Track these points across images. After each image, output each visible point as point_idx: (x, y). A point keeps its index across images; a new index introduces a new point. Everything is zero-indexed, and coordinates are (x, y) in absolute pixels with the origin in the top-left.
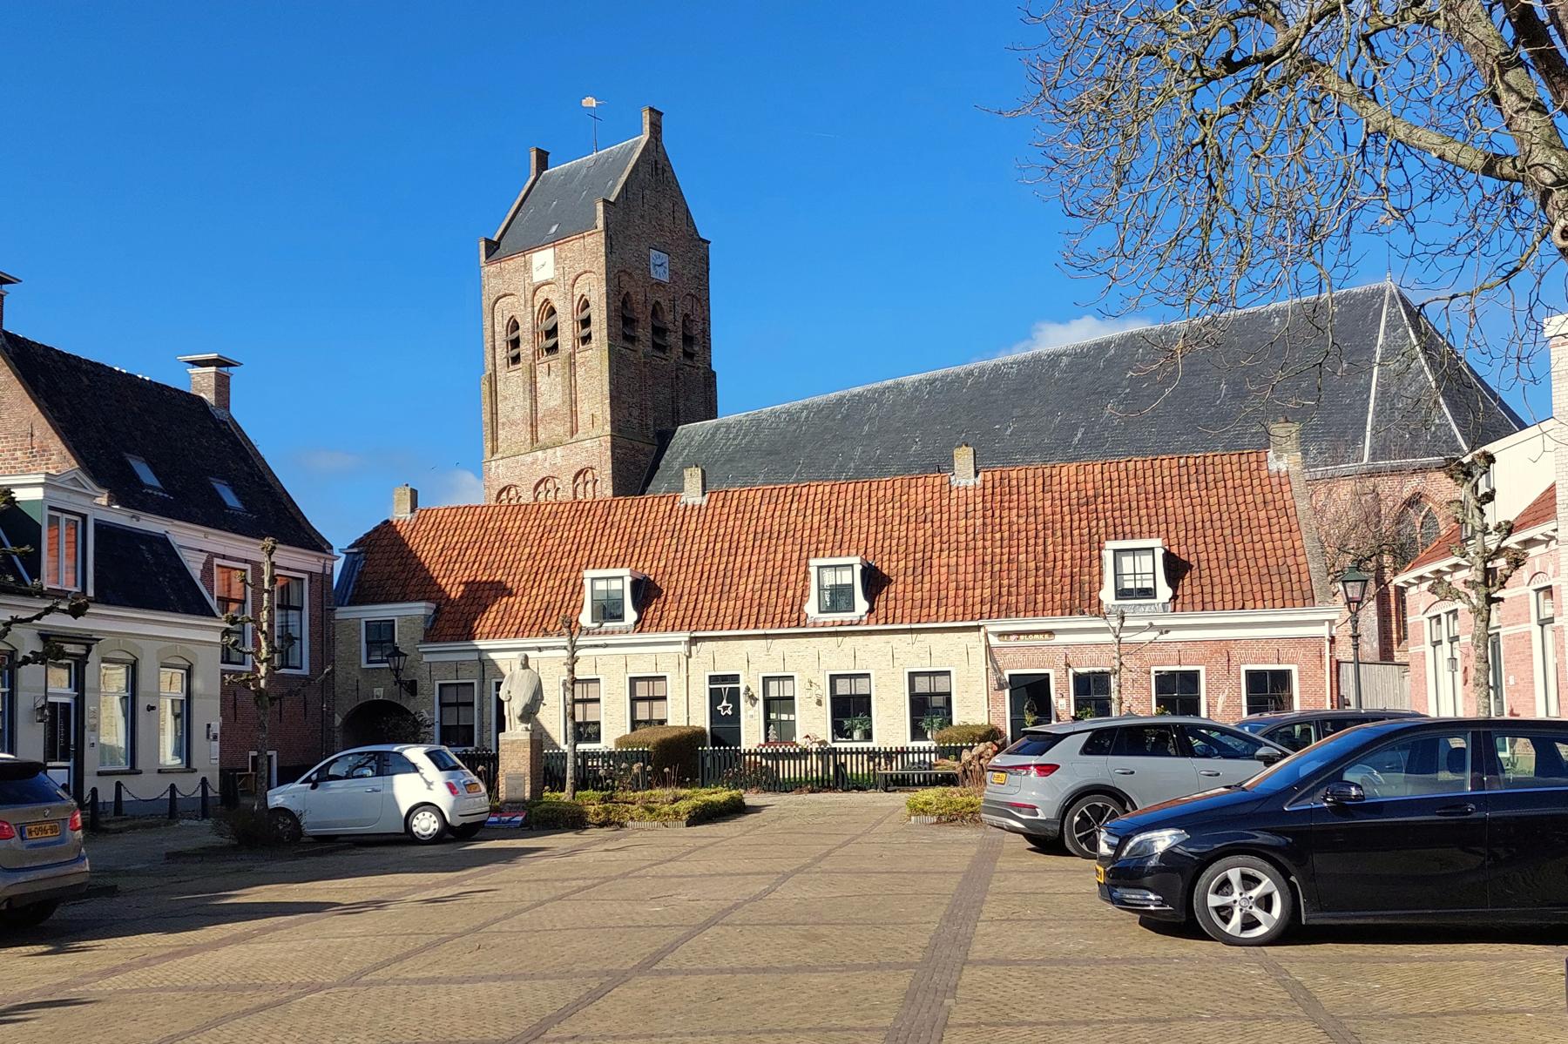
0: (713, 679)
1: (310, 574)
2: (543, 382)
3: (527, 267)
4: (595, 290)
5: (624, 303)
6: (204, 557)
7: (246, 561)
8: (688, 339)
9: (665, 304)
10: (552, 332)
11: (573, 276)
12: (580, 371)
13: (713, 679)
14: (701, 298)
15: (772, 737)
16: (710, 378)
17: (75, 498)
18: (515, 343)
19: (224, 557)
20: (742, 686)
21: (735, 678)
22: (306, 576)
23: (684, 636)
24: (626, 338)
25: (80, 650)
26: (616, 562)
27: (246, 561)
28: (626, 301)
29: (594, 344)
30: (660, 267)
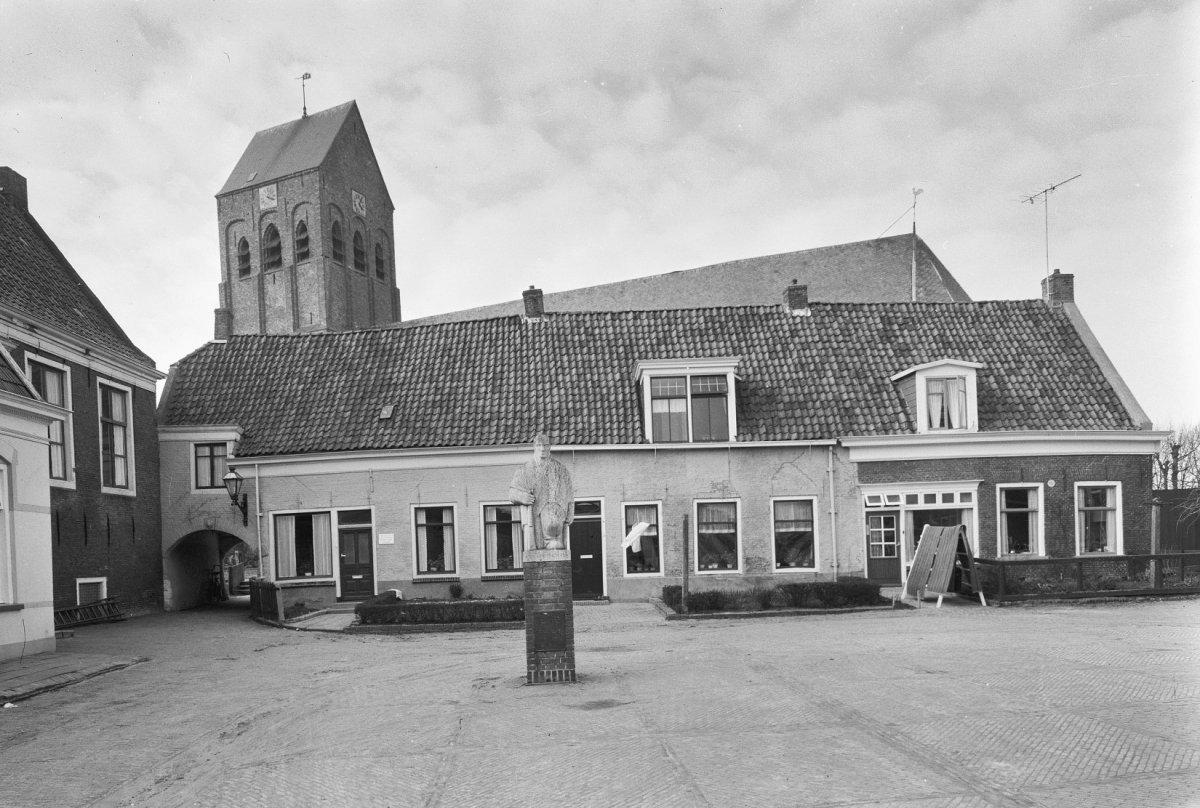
2: (270, 288)
4: (312, 215)
5: (334, 230)
7: (64, 361)
8: (379, 262)
9: (362, 233)
10: (277, 250)
11: (293, 206)
12: (301, 280)
14: (387, 233)
16: (395, 295)
19: (37, 351)
28: (336, 227)
30: (359, 205)
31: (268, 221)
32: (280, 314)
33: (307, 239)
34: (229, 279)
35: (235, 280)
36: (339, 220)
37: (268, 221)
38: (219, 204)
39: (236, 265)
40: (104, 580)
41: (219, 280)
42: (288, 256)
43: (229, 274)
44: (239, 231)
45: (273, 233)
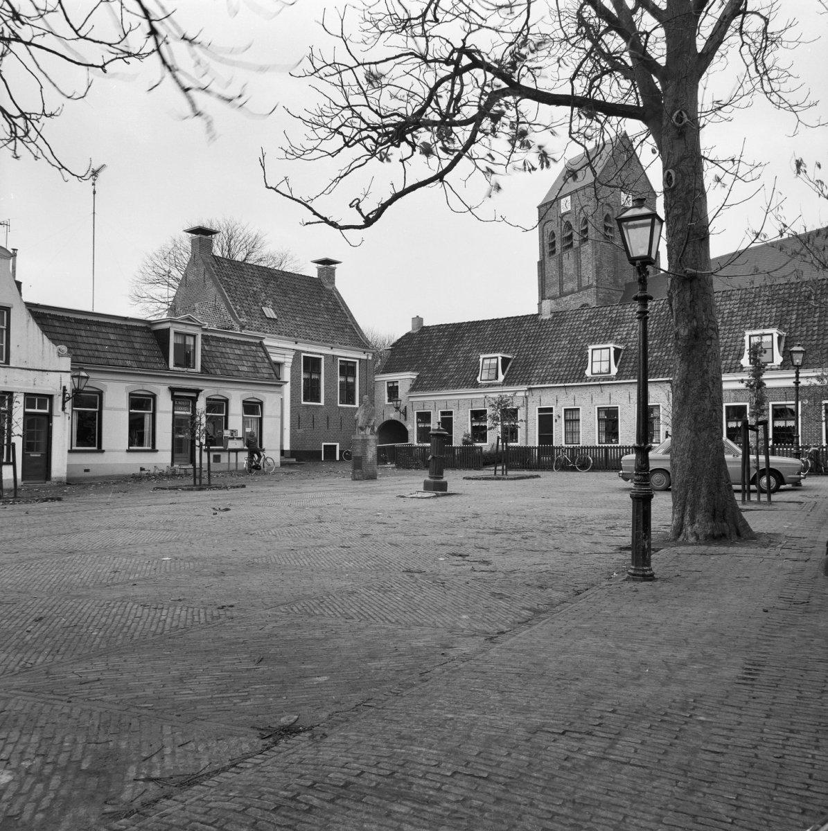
0: (541, 410)
1: (360, 359)
3: (559, 205)
6: (293, 353)
7: (321, 354)
10: (570, 237)
12: (582, 256)
13: (541, 410)
15: (570, 441)
17: (189, 327)
18: (553, 244)
20: (554, 414)
21: (551, 410)
22: (358, 361)
23: (525, 387)
24: (607, 237)
25: (194, 395)
26: (495, 351)
27: (321, 354)
28: (607, 218)
29: (590, 242)
31: (565, 219)
32: (571, 280)
33: (587, 228)
34: (544, 259)
35: (547, 259)
36: (610, 213)
37: (565, 219)
38: (539, 212)
39: (547, 249)
40: (338, 444)
41: (538, 260)
42: (576, 244)
43: (544, 255)
44: (551, 227)
45: (569, 226)
